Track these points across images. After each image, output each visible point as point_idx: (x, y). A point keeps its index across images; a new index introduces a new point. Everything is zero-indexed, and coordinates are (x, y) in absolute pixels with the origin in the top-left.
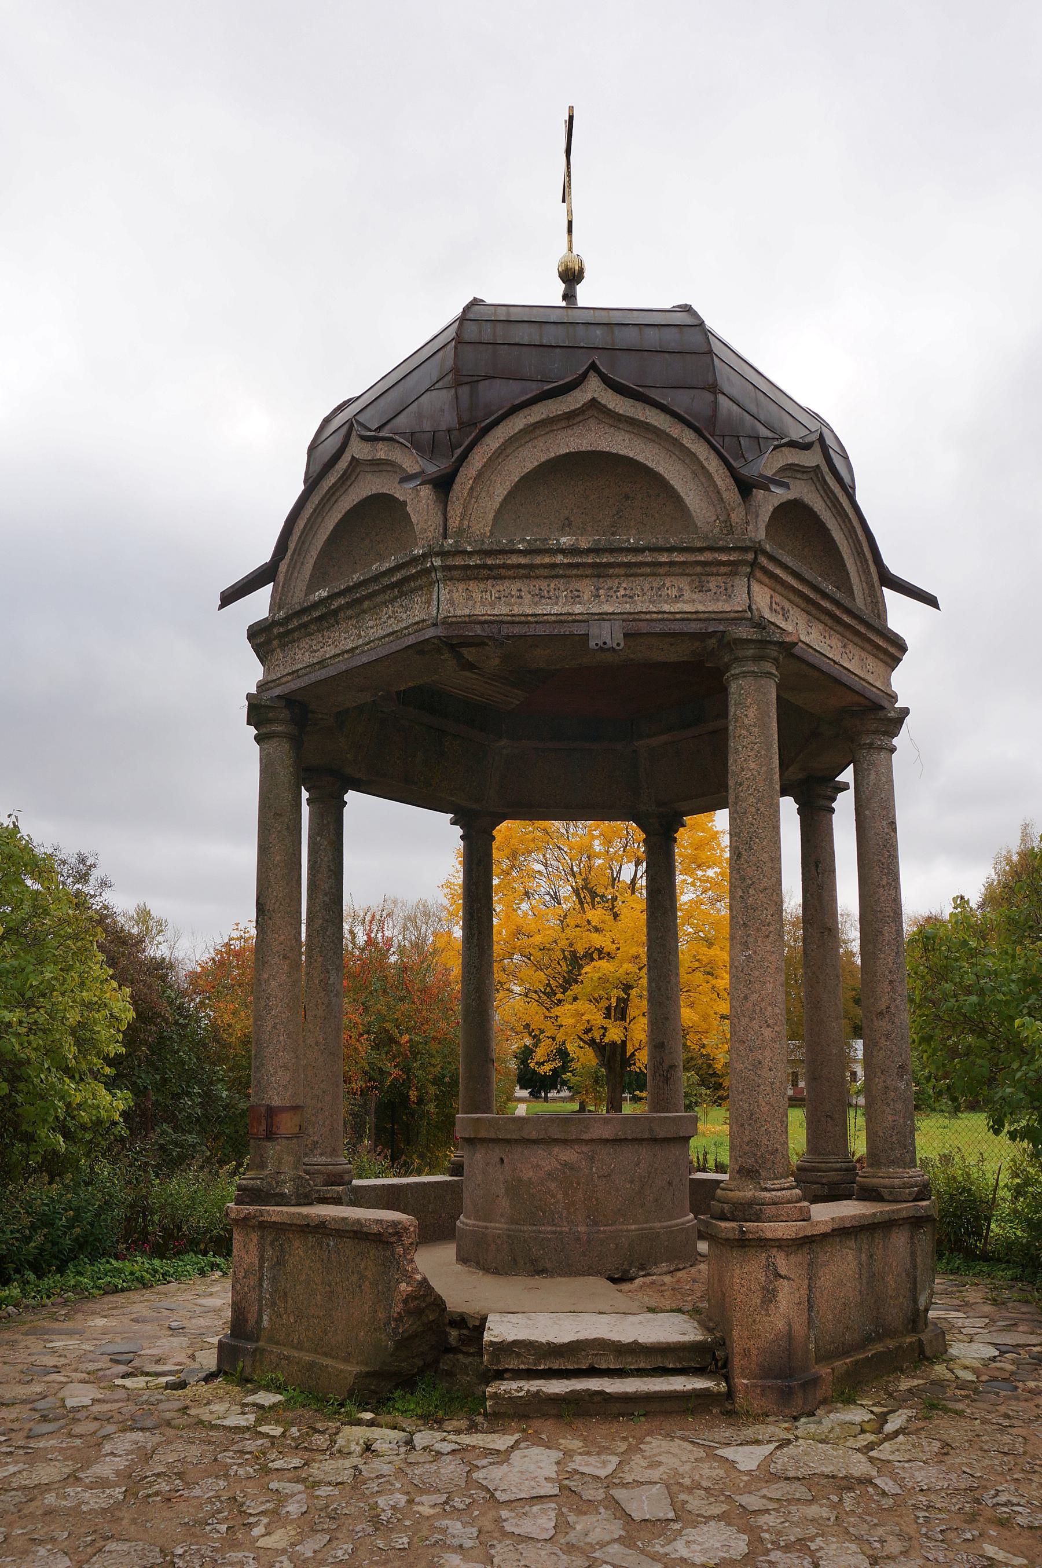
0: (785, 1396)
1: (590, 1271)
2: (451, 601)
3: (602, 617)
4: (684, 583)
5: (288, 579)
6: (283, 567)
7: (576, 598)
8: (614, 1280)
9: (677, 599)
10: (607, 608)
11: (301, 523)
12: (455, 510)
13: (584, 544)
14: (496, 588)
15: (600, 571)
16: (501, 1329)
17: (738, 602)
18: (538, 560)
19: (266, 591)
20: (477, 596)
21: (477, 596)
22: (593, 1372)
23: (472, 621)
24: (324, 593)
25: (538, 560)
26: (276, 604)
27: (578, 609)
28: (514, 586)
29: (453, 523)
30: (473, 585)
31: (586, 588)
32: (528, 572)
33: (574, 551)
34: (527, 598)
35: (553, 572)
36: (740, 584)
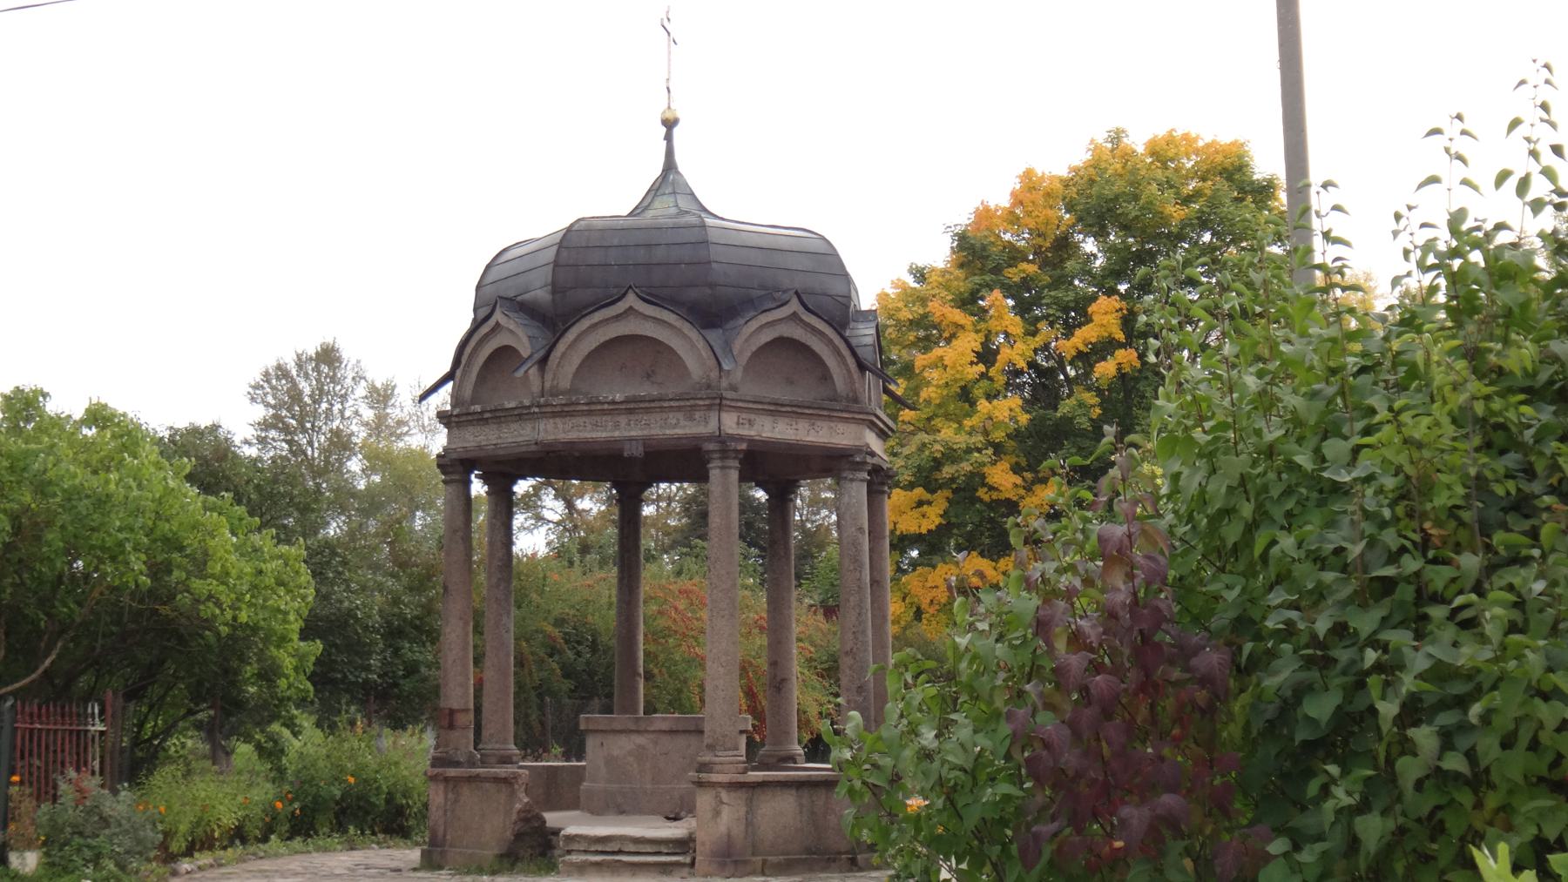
0: (722, 865)
1: (653, 812)
2: (546, 431)
3: (631, 439)
4: (680, 415)
5: (461, 381)
6: (458, 373)
7: (617, 426)
8: (668, 818)
9: (675, 426)
10: (633, 433)
11: (468, 350)
12: (549, 376)
13: (618, 397)
14: (570, 422)
15: (630, 411)
16: (572, 830)
17: (711, 427)
18: (593, 407)
19: (449, 386)
20: (560, 426)
21: (560, 426)
22: (620, 852)
23: (556, 442)
24: (478, 408)
25: (593, 407)
26: (456, 398)
27: (617, 434)
28: (580, 420)
29: (548, 385)
30: (558, 420)
31: (623, 420)
32: (590, 413)
33: (613, 402)
34: (589, 427)
35: (603, 412)
36: (713, 417)
